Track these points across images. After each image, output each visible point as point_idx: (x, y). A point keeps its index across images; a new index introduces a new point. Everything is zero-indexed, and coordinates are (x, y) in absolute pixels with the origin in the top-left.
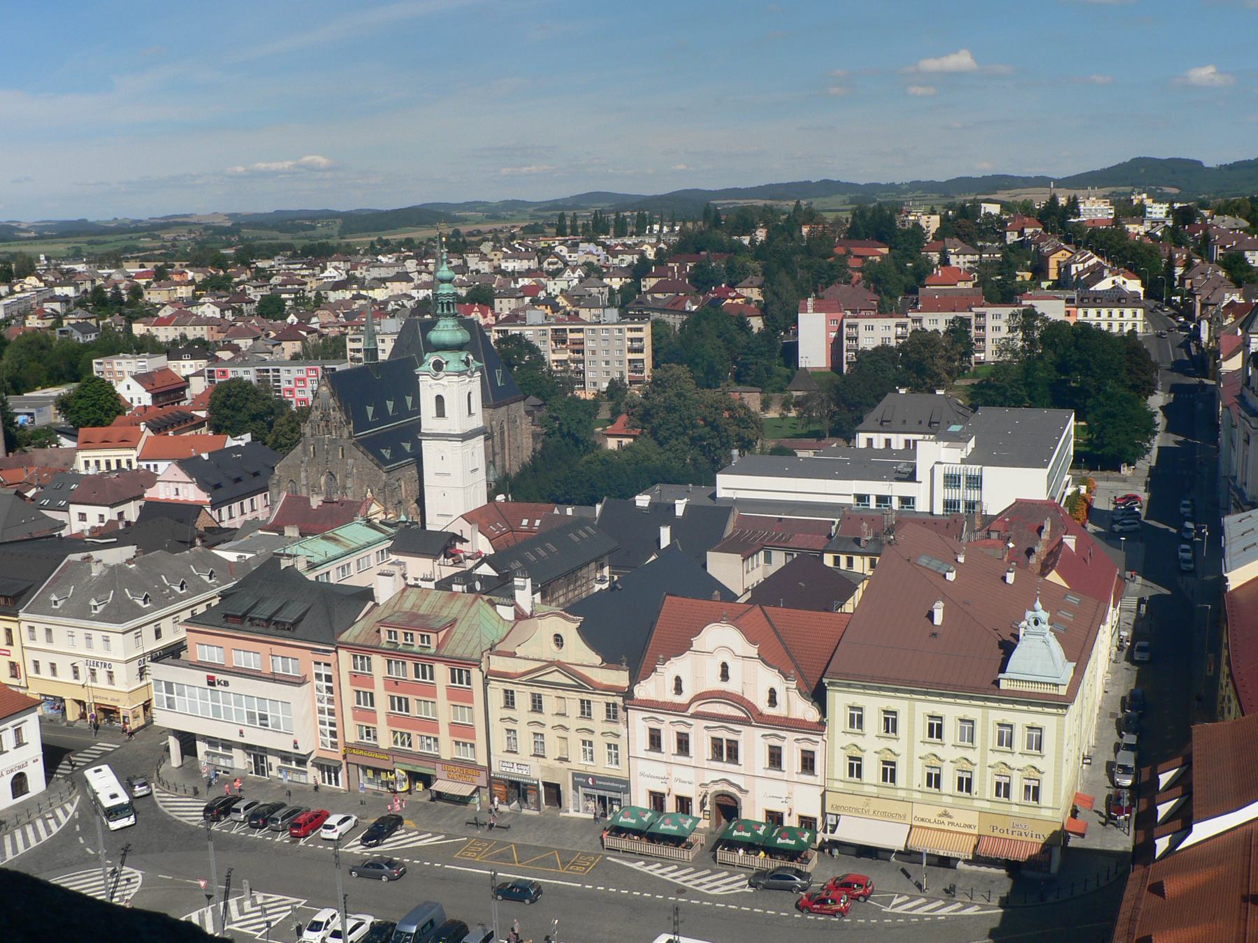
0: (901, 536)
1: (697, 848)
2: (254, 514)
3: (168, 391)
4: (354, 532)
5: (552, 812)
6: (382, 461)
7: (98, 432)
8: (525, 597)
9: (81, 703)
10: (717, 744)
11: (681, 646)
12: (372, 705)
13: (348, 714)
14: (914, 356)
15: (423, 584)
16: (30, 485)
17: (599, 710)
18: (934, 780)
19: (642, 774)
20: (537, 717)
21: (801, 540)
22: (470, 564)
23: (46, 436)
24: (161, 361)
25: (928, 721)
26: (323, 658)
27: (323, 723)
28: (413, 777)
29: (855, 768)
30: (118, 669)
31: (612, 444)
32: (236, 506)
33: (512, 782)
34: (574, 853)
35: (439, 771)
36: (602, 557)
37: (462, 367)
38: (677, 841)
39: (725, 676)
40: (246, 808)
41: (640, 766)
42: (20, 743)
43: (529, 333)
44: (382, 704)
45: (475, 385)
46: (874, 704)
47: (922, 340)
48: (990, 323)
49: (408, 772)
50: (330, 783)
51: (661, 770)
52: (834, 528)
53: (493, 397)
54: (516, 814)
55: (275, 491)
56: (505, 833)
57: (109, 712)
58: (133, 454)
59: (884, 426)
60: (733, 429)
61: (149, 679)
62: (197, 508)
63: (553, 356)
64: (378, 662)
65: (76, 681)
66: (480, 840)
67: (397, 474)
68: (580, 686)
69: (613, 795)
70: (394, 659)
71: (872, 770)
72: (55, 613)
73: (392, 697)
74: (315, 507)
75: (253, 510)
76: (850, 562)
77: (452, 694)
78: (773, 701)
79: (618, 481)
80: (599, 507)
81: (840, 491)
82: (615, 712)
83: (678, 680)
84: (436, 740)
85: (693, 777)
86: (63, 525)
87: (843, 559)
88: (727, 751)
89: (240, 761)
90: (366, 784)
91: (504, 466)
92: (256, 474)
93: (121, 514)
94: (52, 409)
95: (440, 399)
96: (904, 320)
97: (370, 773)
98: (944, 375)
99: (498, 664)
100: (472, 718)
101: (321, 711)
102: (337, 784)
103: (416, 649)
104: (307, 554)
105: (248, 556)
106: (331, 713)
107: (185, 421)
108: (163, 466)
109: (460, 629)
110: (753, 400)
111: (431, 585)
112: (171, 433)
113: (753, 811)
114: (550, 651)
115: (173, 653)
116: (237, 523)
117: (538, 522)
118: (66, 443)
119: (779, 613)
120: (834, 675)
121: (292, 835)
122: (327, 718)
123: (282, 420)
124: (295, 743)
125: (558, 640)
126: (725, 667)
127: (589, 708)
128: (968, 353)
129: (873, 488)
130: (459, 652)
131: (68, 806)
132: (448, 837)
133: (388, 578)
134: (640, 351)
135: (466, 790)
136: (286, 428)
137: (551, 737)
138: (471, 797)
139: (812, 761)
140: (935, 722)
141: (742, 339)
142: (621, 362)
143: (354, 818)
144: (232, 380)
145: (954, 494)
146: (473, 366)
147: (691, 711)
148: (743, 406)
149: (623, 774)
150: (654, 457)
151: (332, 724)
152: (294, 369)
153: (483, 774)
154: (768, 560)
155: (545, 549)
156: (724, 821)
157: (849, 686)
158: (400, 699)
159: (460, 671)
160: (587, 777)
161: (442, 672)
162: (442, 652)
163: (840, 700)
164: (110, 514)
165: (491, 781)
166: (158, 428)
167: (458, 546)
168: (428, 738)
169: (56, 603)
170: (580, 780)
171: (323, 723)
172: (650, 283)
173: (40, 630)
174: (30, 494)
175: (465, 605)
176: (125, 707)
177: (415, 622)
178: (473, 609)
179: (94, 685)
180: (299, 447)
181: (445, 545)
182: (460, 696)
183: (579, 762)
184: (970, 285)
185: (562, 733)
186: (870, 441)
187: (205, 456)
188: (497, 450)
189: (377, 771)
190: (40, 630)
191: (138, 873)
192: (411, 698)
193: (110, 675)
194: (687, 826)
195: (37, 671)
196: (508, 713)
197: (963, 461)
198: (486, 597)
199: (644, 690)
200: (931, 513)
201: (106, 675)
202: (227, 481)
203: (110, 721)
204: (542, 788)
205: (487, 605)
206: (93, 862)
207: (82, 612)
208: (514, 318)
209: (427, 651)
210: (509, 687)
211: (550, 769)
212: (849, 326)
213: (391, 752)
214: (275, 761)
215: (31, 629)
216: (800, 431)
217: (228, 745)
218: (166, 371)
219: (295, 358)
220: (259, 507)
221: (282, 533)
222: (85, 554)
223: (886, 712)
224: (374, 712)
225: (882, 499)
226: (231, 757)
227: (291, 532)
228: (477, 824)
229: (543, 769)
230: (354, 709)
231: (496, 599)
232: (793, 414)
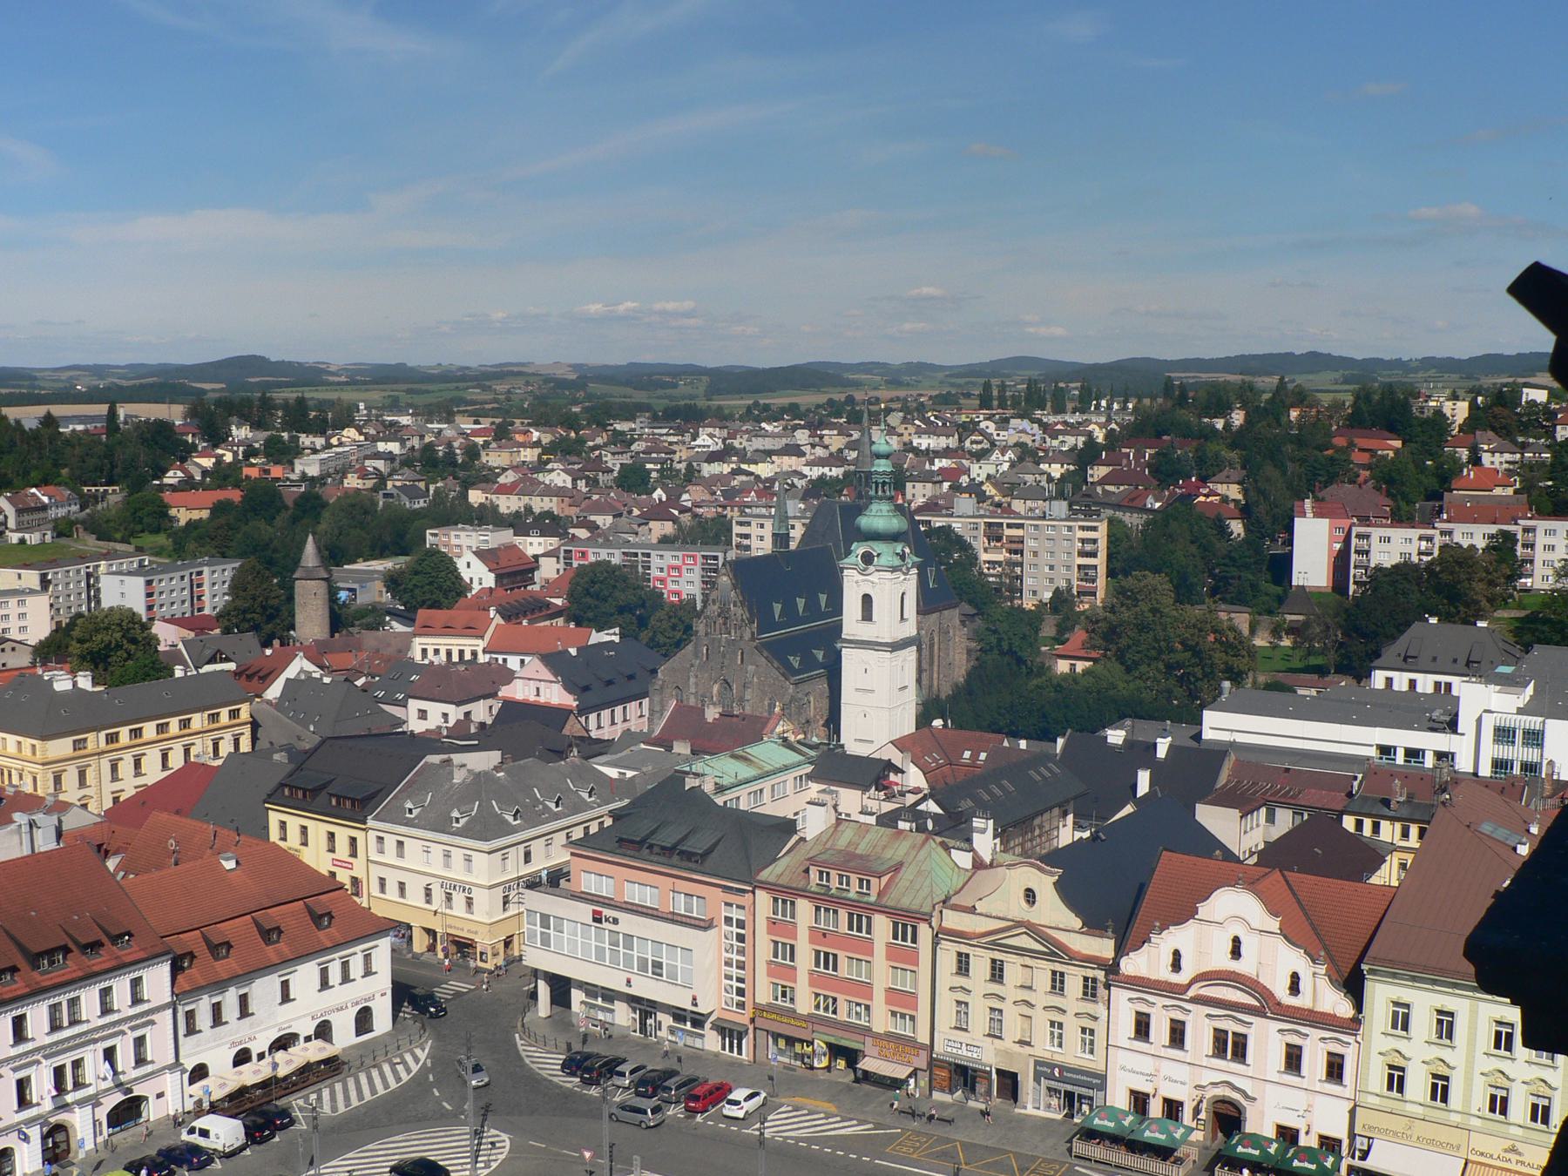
0: (1459, 796)
1: (1188, 1165)
2: (626, 725)
3: (513, 572)
4: (768, 752)
5: (1005, 1107)
6: (788, 671)
7: (440, 616)
8: (985, 841)
9: (431, 933)
10: (1220, 1038)
11: (1184, 913)
12: (792, 959)
13: (761, 969)
14: (1445, 577)
15: (863, 819)
16: (360, 674)
17: (1074, 985)
18: (1499, 1105)
19: (1123, 1068)
20: (995, 988)
21: (1314, 797)
22: (910, 799)
23: (374, 617)
24: (505, 536)
25: (1494, 1028)
27: (729, 977)
28: (835, 1051)
29: (1396, 1080)
30: (479, 896)
31: (1063, 666)
32: (606, 714)
33: (958, 1066)
34: (1034, 1158)
35: (869, 1046)
36: (1067, 801)
37: (897, 562)
38: (1164, 1153)
39: (1236, 952)
40: (632, 1073)
41: (1119, 1058)
42: (368, 972)
43: (957, 525)
45: (910, 584)
46: (1424, 1002)
47: (1455, 557)
48: (1541, 540)
49: (829, 1045)
50: (731, 1050)
51: (1147, 1064)
52: (1356, 784)
53: (928, 602)
54: (961, 1106)
55: (657, 699)
56: (948, 1128)
57: (463, 947)
58: (480, 645)
59: (1408, 662)
60: (1219, 657)
61: (513, 910)
62: (557, 715)
63: (988, 555)
64: (804, 908)
65: (427, 906)
66: (918, 1133)
67: (806, 687)
68: (1053, 954)
69: (1084, 1091)
70: (823, 906)
71: (1418, 1085)
72: (409, 823)
73: (818, 953)
74: (710, 720)
75: (625, 720)
76: (1376, 828)
77: (892, 953)
78: (1295, 988)
79: (1082, 710)
80: (1060, 741)
81: (1358, 740)
82: (1094, 988)
83: (1177, 955)
84: (868, 1008)
85: (1187, 1077)
87: (1368, 823)
88: (1232, 1047)
89: (623, 1016)
90: (776, 1056)
91: (931, 687)
92: (631, 677)
93: (467, 714)
94: (379, 585)
95: (867, 600)
96: (1430, 532)
97: (782, 1043)
98: (1484, 603)
99: (952, 920)
100: (915, 983)
101: (728, 963)
103: (852, 895)
104: (714, 774)
105: (630, 774)
106: (741, 966)
107: (537, 608)
108: (513, 662)
109: (907, 874)
110: (1242, 620)
111: (872, 820)
112: (525, 623)
113: (1261, 1122)
114: (1019, 910)
116: (606, 733)
117: (983, 756)
118: (398, 627)
119: (1307, 882)
120: (1375, 960)
121: (687, 1109)
122: (734, 971)
123: (660, 614)
125: (1030, 896)
126: (1236, 942)
127: (1062, 982)
128: (1513, 577)
129: (1402, 739)
130: (905, 902)
131: (418, 1051)
132: (878, 1126)
133: (813, 811)
134: (1093, 555)
135: (901, 1072)
136: (665, 625)
137: (1011, 1016)
138: (905, 1082)
139: (1341, 1067)
140: (1504, 1030)
141: (1221, 547)
142: (1068, 568)
143: (763, 1095)
144: (598, 563)
145: (1505, 752)
146: (909, 562)
147: (1191, 993)
148: (1233, 629)
149: (1099, 1067)
150: (1121, 685)
151: (740, 980)
152: (668, 554)
153: (924, 1054)
154: (1271, 819)
155: (1001, 787)
156: (1220, 1135)
157: (1394, 976)
158: (827, 955)
159: (905, 926)
160: (1053, 1066)
161: (882, 926)
162: (884, 901)
163: (1381, 994)
164: (455, 713)
165: (933, 1063)
166: (510, 614)
167: (892, 777)
168: (858, 1004)
169: (410, 811)
170: (1044, 1069)
171: (729, 977)
172: (1098, 472)
173: (390, 841)
174: (359, 683)
175: (913, 847)
176: (484, 941)
177: (851, 862)
178: (923, 853)
179: (448, 911)
180: (690, 647)
181: (873, 774)
182: (902, 957)
183: (1043, 1047)
184: (1510, 491)
185: (1026, 1010)
186: (1389, 681)
187: (573, 651)
188: (925, 666)
189: (791, 1041)
190: (390, 841)
191: (505, 1137)
192: (841, 955)
194: (1178, 1136)
195: (383, 890)
196: (961, 981)
197: (1520, 711)
198: (939, 839)
199: (1133, 964)
200: (1475, 774)
202: (598, 683)
203: (464, 956)
204: (994, 1076)
205: (940, 849)
206: (450, 1119)
207: (442, 825)
208: (932, 507)
209: (866, 899)
210: (964, 949)
211: (1007, 1054)
212: (1359, 536)
213: (809, 1018)
214: (666, 1020)
215: (380, 839)
216: (1297, 664)
217: (610, 995)
218: (512, 548)
219: (665, 541)
220: (634, 716)
221: (669, 748)
222: (445, 757)
223: (1440, 1012)
224: (795, 968)
225: (1412, 753)
226: (612, 1011)
227: (682, 748)
228: (913, 1114)
229: (998, 1052)
230: (769, 963)
231: (951, 842)
232: (1286, 642)
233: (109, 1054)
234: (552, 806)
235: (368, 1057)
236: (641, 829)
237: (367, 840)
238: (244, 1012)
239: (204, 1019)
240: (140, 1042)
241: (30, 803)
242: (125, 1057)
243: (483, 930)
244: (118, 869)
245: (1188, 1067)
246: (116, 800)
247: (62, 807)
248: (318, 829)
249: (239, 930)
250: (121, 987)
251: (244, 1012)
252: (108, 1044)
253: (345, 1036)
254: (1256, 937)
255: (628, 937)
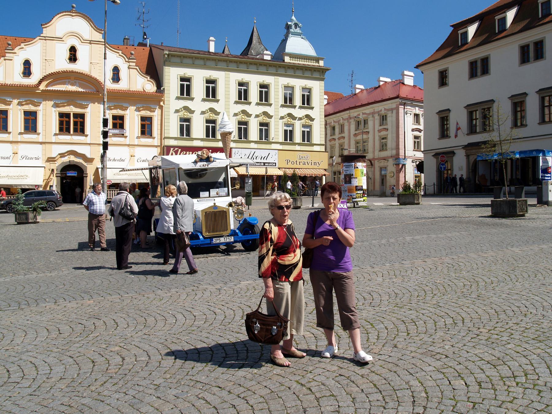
10: (64, 117)
78: (116, 78)
83: (27, 64)
88: (72, 124)
126: (73, 50)
163: (172, 75)
245: (40, 146)
254: (87, 47)
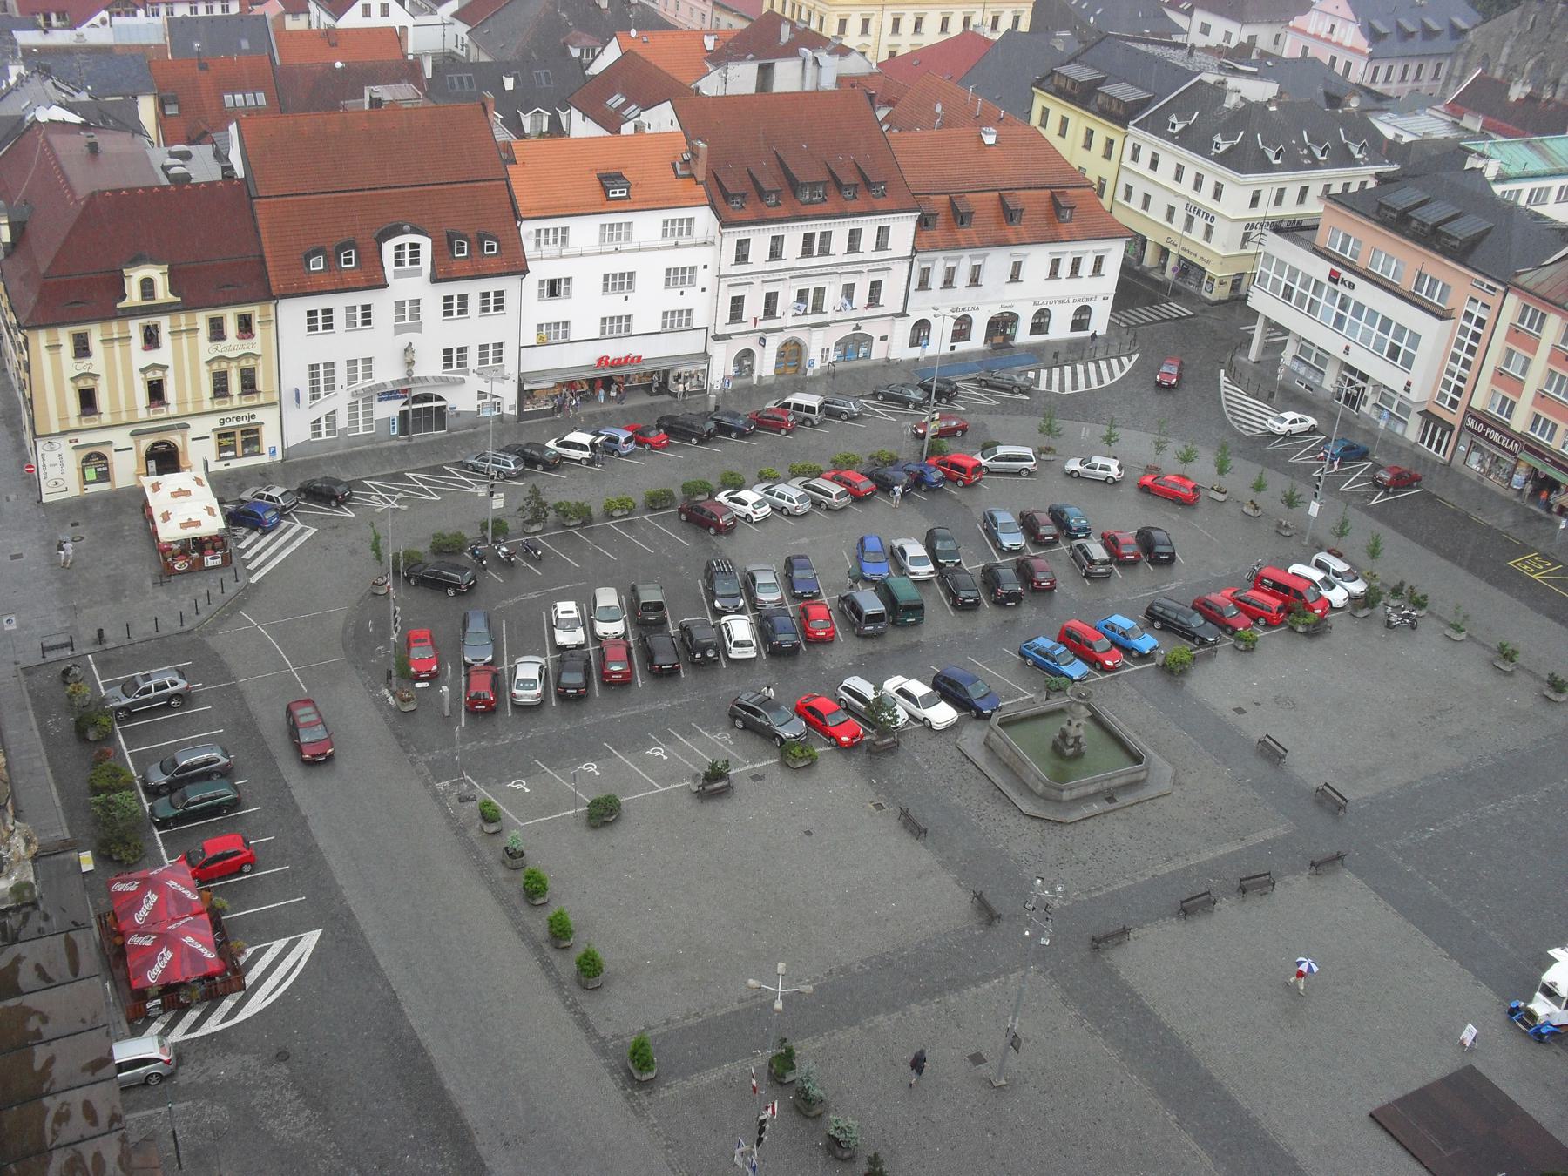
2: (1416, 85)
26: (1482, 297)
42: (1097, 270)
44: (1535, 379)
50: (1430, 445)
65: (1167, 224)
72: (1170, 138)
86: (1181, 31)
93: (1252, 38)
101: (1455, 358)
102: (1437, 450)
106: (1466, 364)
115: (1295, 230)
122: (1458, 368)
124: (1409, 384)
131: (1125, 360)
151: (1461, 379)
169: (1173, 126)
173: (1145, 156)
179: (1186, 234)
193: (1209, 230)
195: (1128, 197)
201: (1203, 228)
213: (1521, 438)
233: (849, 290)
234: (1317, 152)
235: (1076, 352)
236: (1403, 198)
237: (1123, 149)
238: (974, 281)
239: (937, 279)
240: (876, 287)
241: (816, 41)
242: (862, 294)
243: (1215, 261)
244: (886, 119)
246: (892, 54)
247: (844, 51)
248: (1080, 121)
249: (983, 203)
250: (869, 228)
251: (974, 281)
252: (848, 280)
253: (1060, 330)
255: (1359, 307)
